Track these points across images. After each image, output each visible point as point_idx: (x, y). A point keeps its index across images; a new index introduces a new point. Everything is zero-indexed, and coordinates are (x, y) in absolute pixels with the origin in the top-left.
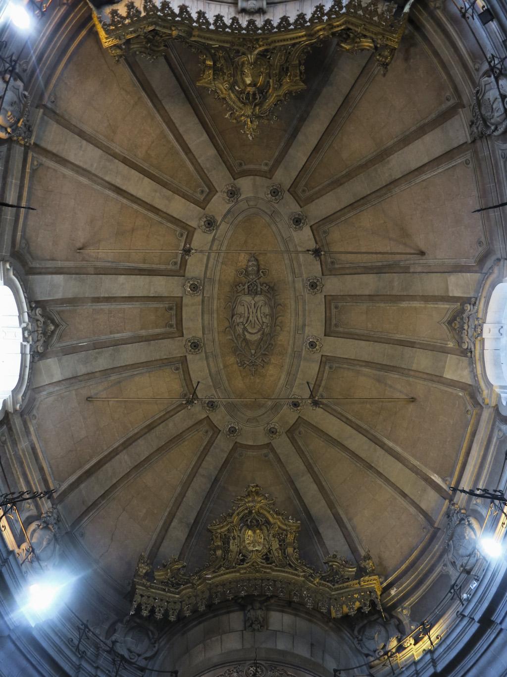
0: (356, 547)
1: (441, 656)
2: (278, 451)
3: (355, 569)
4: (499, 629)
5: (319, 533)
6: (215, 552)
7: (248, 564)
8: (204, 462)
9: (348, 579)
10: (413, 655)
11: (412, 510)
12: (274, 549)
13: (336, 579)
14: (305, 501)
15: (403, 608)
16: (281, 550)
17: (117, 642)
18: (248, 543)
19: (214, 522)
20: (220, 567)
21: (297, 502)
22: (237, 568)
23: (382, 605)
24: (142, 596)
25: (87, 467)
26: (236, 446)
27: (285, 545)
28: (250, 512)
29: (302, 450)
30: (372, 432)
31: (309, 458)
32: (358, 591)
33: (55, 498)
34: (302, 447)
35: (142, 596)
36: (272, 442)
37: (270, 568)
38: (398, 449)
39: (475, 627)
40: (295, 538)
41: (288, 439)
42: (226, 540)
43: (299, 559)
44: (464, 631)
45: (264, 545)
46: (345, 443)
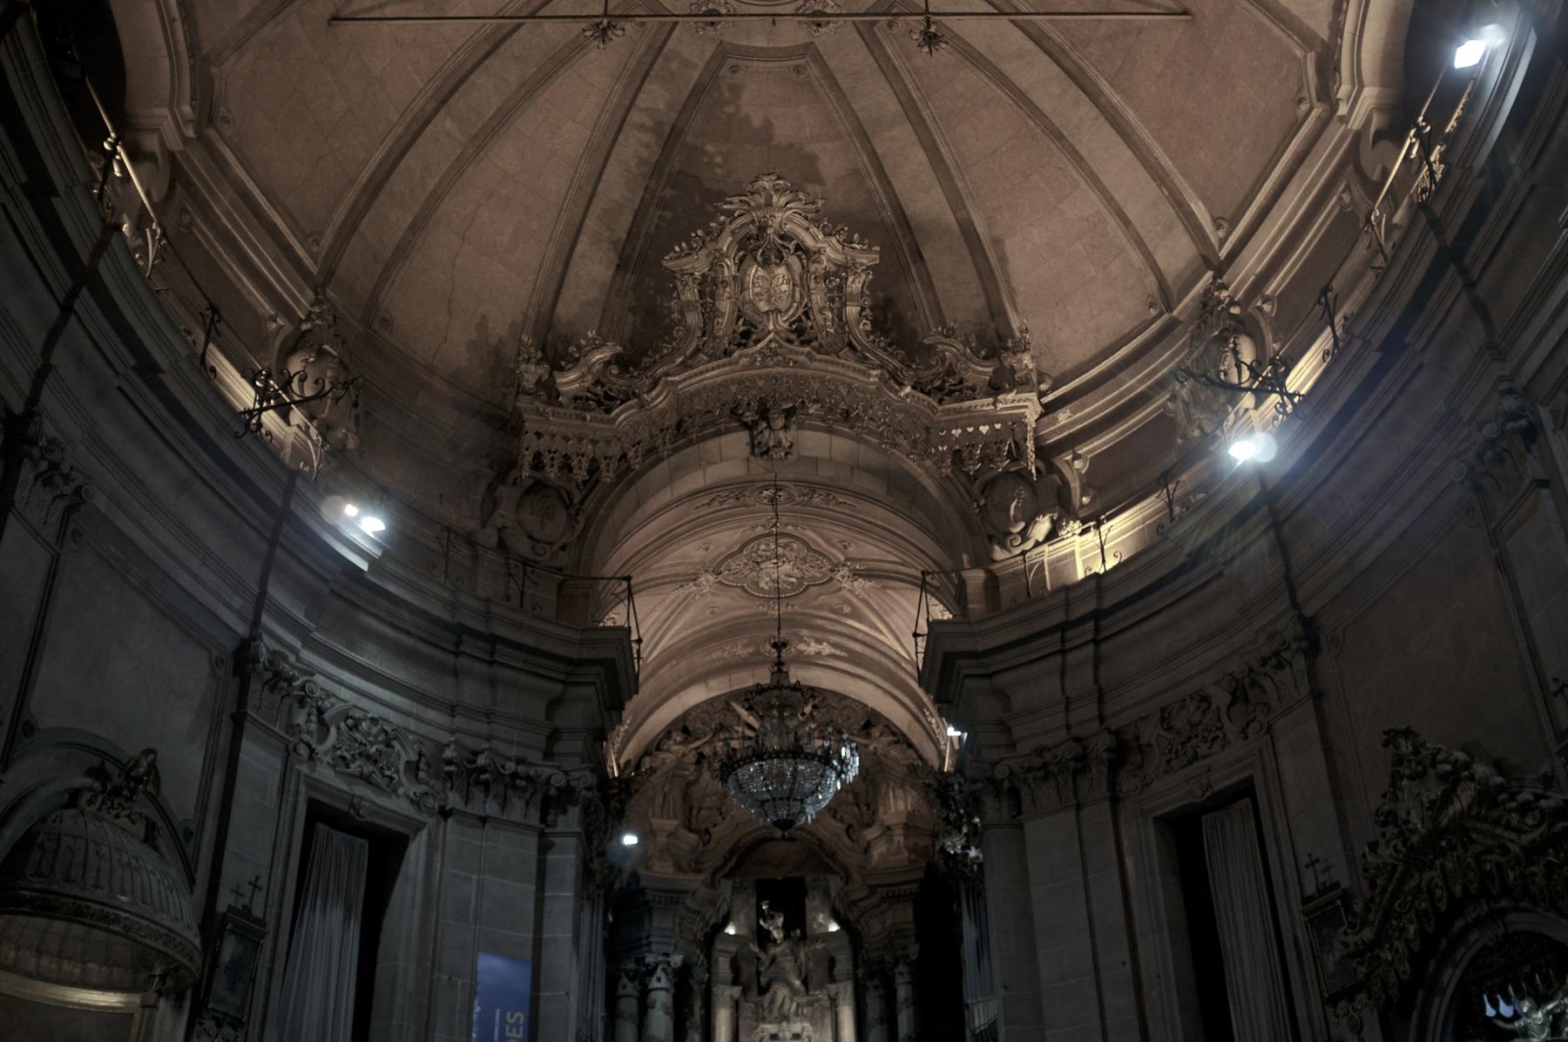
0: (1002, 305)
2: (832, 64)
3: (990, 369)
5: (922, 258)
8: (641, 95)
9: (973, 389)
10: (1073, 553)
11: (1136, 258)
12: (815, 308)
13: (947, 384)
14: (897, 186)
15: (1076, 457)
16: (831, 309)
17: (506, 527)
19: (677, 249)
21: (875, 183)
23: (1037, 440)
24: (539, 435)
25: (364, 177)
26: (723, 53)
28: (762, 228)
29: (895, 67)
30: (1075, 56)
31: (910, 86)
32: (990, 419)
33: (315, 273)
34: (894, 59)
35: (539, 435)
36: (816, 42)
37: (808, 354)
38: (1131, 115)
41: (858, 37)
42: (709, 286)
43: (871, 333)
46: (1007, 68)
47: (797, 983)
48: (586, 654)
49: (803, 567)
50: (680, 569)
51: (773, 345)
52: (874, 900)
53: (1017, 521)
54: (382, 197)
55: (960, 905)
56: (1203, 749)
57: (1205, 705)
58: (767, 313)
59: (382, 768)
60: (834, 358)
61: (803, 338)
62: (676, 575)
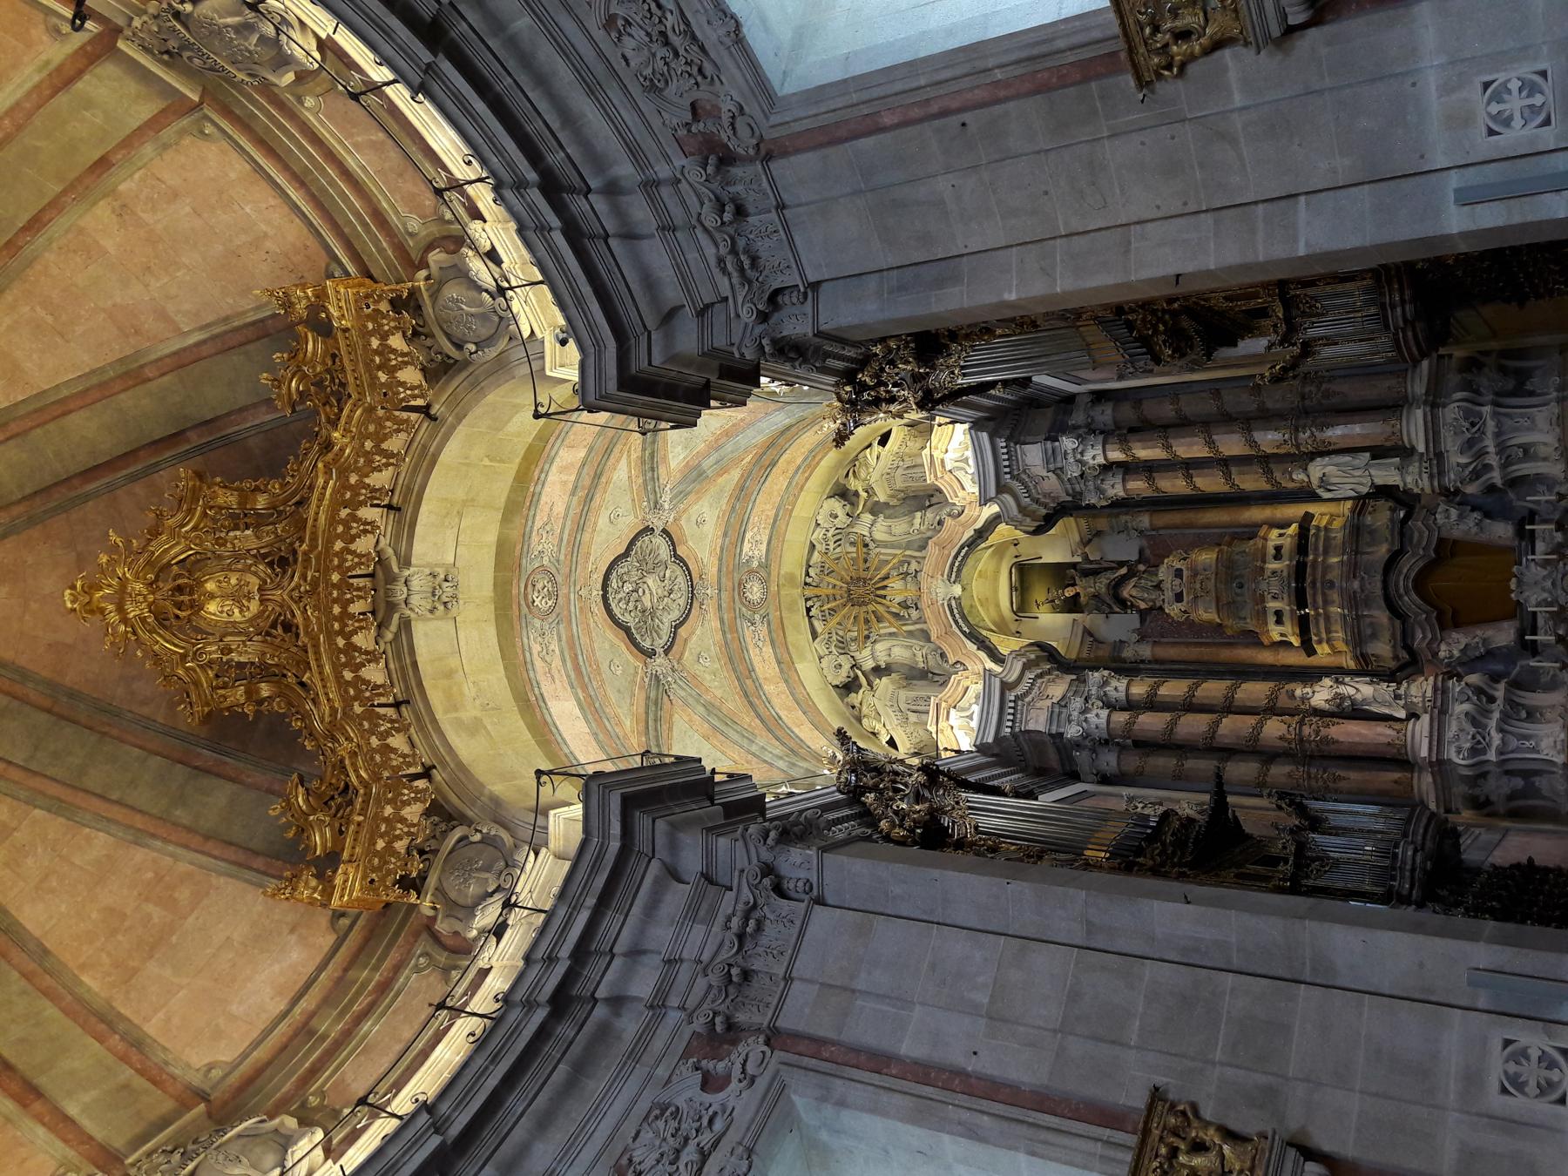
1: (511, 165)
4: (450, 8)
6: (265, 699)
7: (298, 613)
9: (334, 356)
18: (241, 612)
20: (302, 684)
22: (306, 640)
27: (245, 515)
39: (446, 67)
40: (225, 487)
42: (229, 672)
43: (284, 479)
44: (453, 94)
45: (247, 569)
47: (1124, 571)
48: (616, 829)
49: (650, 562)
50: (640, 697)
51: (296, 594)
52: (1016, 485)
53: (481, 304)
54: (42, 1081)
55: (992, 384)
56: (671, 20)
57: (620, 22)
58: (262, 601)
59: (697, 1131)
60: (310, 523)
61: (291, 559)
62: (648, 698)
